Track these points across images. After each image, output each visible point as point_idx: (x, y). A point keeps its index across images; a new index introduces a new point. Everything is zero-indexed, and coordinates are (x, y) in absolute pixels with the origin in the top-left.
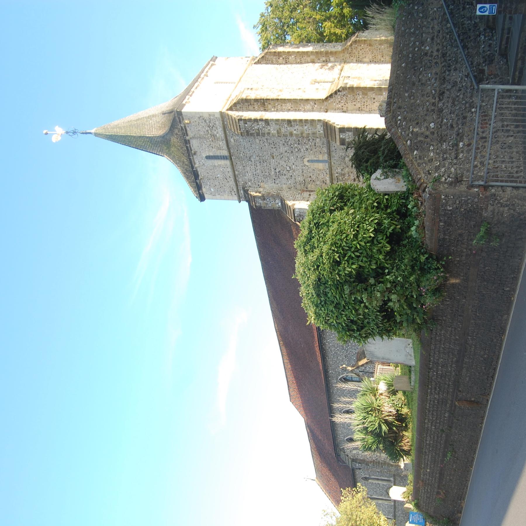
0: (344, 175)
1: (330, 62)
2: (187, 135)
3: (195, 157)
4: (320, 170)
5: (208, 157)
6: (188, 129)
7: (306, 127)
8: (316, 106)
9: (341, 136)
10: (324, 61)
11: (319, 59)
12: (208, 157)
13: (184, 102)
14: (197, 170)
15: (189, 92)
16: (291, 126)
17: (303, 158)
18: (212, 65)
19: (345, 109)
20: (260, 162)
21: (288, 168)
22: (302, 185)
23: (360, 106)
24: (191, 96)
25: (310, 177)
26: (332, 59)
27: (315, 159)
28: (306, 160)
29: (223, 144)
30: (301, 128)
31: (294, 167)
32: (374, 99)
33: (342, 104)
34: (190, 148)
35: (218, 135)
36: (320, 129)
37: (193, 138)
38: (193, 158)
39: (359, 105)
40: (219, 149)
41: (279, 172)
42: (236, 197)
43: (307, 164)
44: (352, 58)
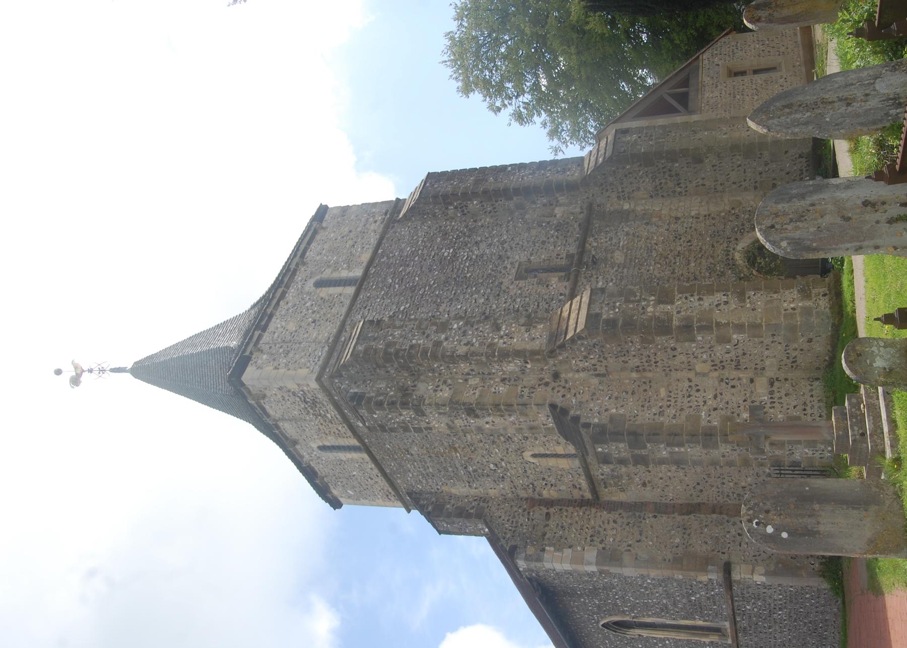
0: (617, 477)
1: (558, 204)
2: (268, 416)
3: (298, 447)
4: (563, 469)
5: (323, 448)
6: (267, 407)
7: (512, 418)
8: (529, 366)
9: (600, 450)
10: (545, 205)
11: (534, 202)
12: (323, 448)
13: (247, 353)
14: (309, 466)
15: (261, 320)
16: (477, 416)
17: (520, 451)
18: (315, 232)
19: (601, 370)
20: (430, 457)
21: (492, 466)
22: (530, 491)
23: (637, 364)
24: (264, 329)
25: (544, 479)
26: (562, 199)
27: (547, 452)
28: (527, 455)
29: (343, 428)
30: (498, 420)
31: (503, 464)
32: (674, 349)
33: (593, 362)
34: (282, 434)
35: (329, 416)
36: (544, 419)
37: (283, 419)
38: (296, 450)
39: (635, 362)
40: (339, 435)
41: (475, 471)
42: (400, 504)
43: (532, 460)
44: (608, 194)
